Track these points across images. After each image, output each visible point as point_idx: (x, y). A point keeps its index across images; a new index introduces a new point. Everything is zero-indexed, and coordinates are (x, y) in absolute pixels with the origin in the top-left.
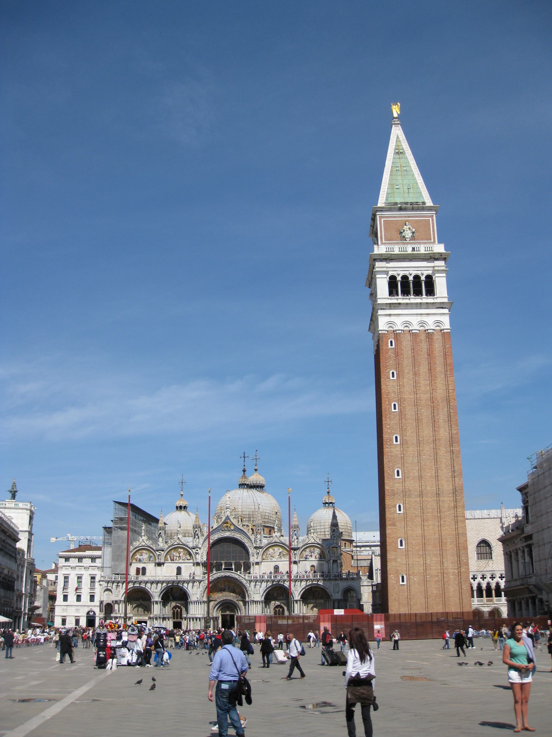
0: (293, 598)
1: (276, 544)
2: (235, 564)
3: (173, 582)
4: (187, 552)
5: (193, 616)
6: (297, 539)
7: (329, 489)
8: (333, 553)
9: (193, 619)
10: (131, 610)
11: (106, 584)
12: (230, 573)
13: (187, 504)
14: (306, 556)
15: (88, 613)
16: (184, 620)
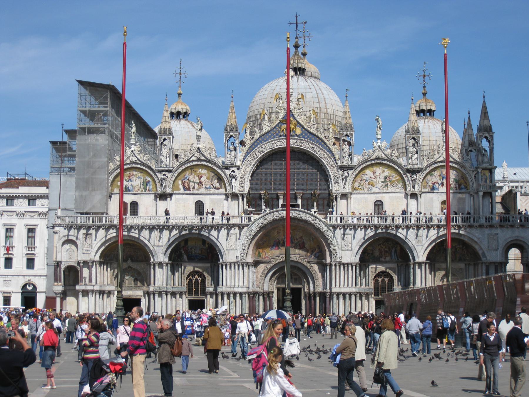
0: (414, 259)
1: (378, 161)
2: (302, 196)
3: (191, 227)
4: (213, 174)
5: (229, 290)
6: (417, 153)
7: (425, 89)
8: (484, 180)
9: (229, 294)
10: (111, 279)
11: (66, 230)
12: (298, 212)
13: (188, 108)
14: (434, 184)
15: (24, 287)
16: (209, 296)
